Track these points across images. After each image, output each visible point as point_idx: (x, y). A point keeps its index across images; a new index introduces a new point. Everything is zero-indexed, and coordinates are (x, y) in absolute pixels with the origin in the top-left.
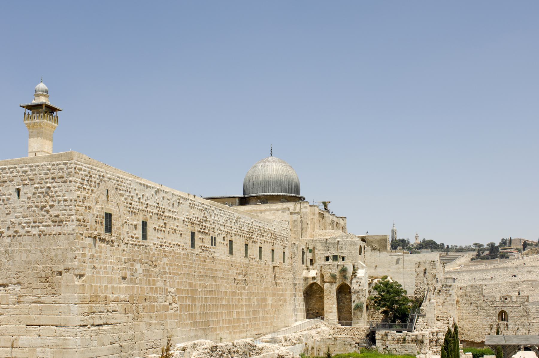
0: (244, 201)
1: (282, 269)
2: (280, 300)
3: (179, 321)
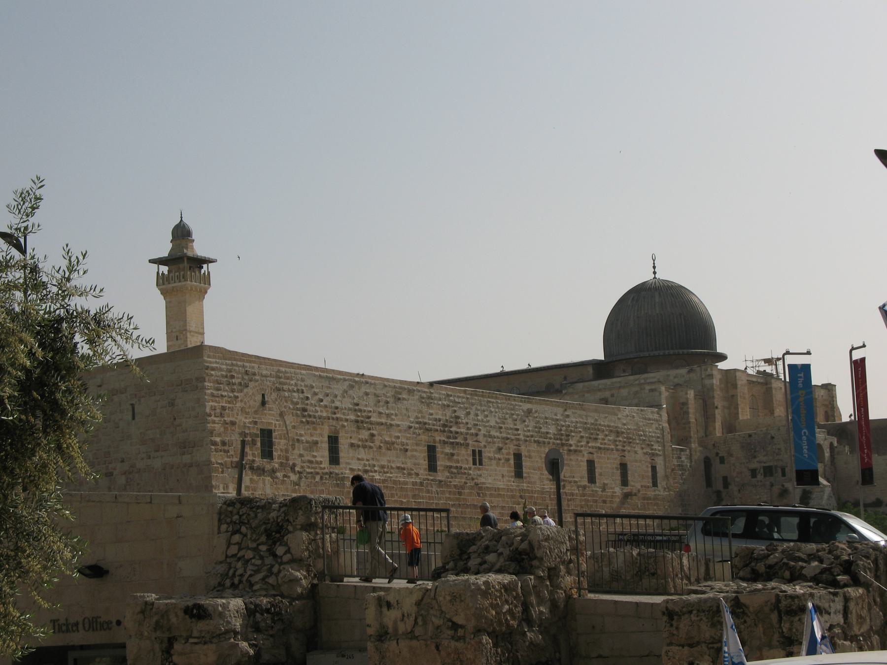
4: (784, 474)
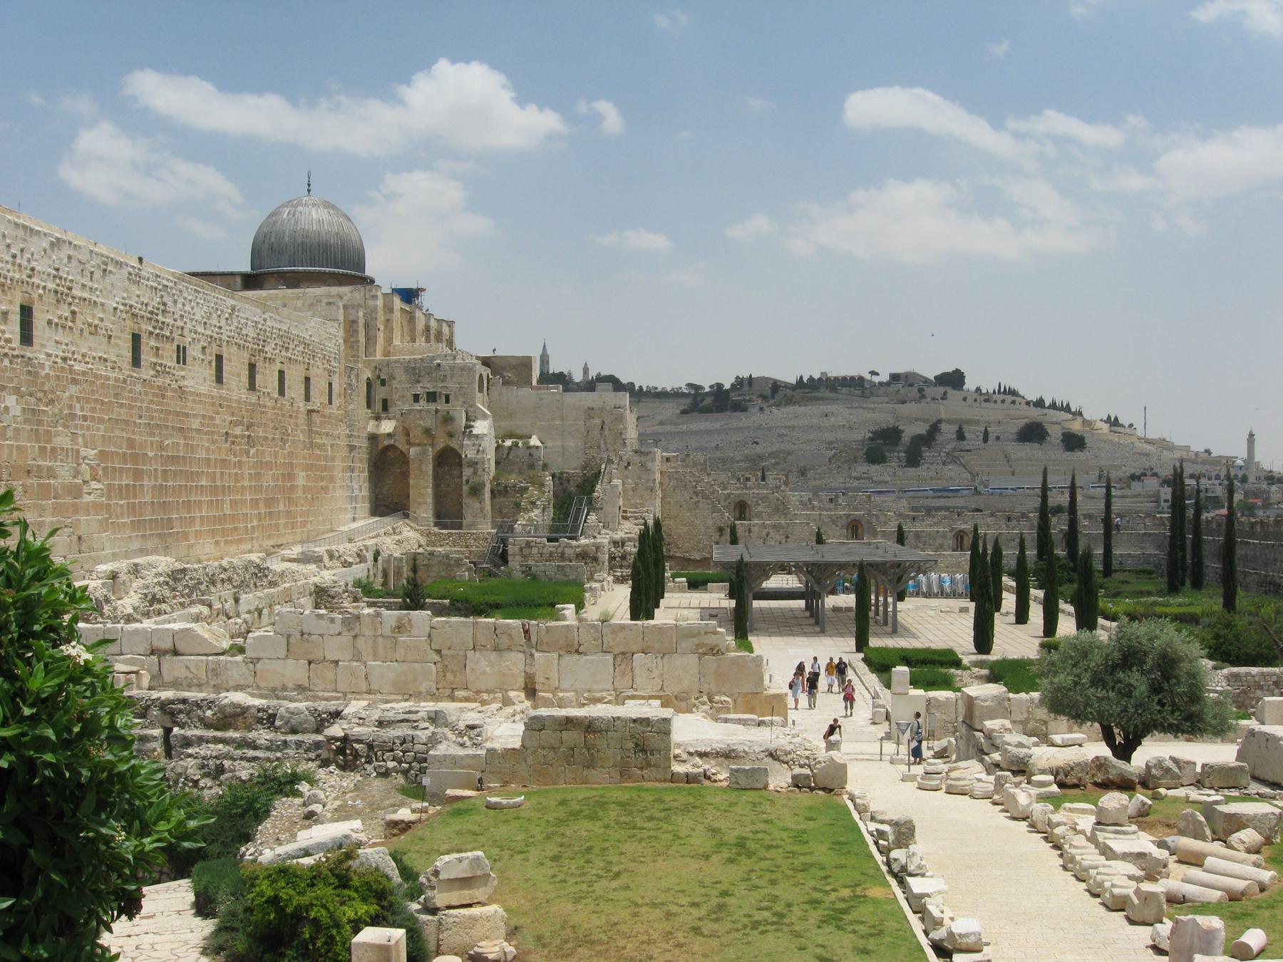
0: (251, 281)
1: (325, 416)
2: (322, 479)
3: (107, 519)
4: (447, 401)
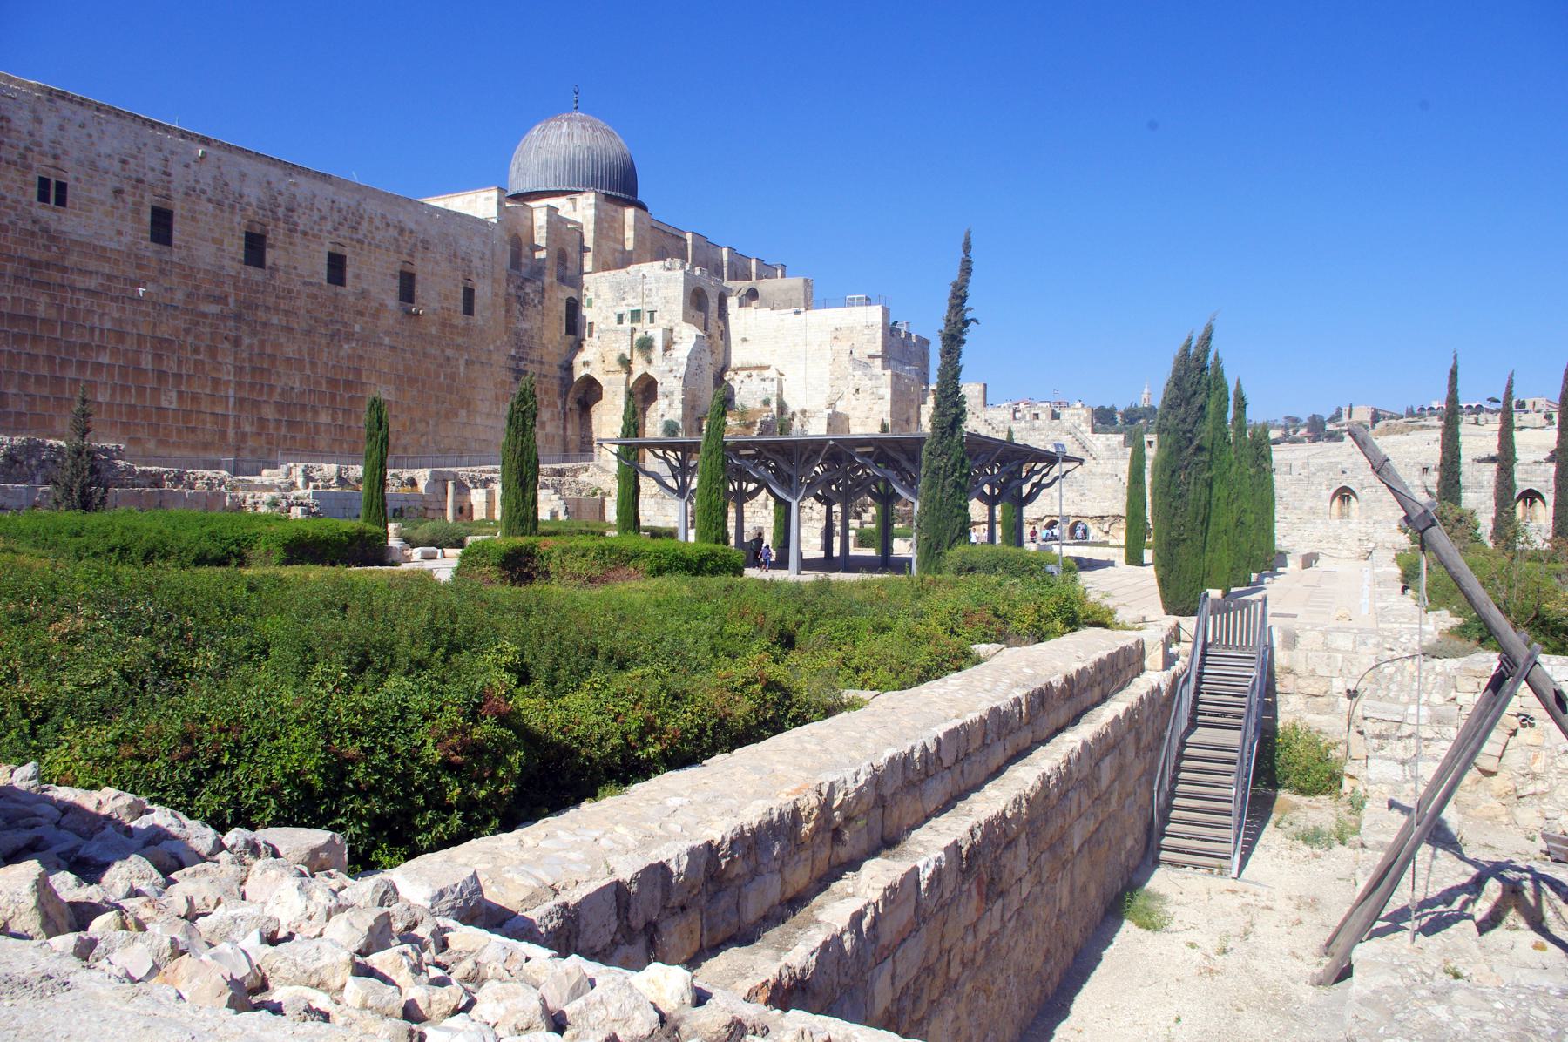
4: (652, 321)
